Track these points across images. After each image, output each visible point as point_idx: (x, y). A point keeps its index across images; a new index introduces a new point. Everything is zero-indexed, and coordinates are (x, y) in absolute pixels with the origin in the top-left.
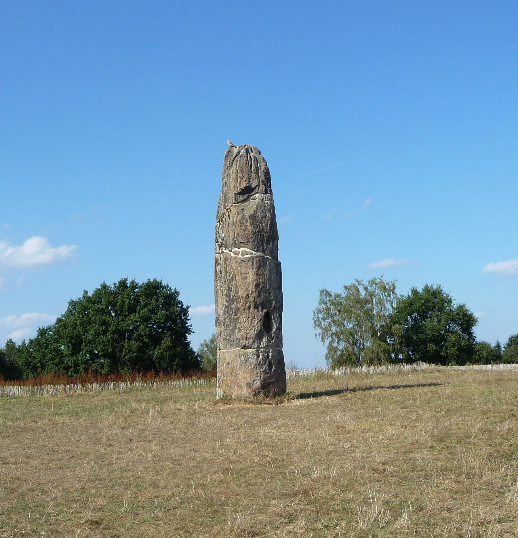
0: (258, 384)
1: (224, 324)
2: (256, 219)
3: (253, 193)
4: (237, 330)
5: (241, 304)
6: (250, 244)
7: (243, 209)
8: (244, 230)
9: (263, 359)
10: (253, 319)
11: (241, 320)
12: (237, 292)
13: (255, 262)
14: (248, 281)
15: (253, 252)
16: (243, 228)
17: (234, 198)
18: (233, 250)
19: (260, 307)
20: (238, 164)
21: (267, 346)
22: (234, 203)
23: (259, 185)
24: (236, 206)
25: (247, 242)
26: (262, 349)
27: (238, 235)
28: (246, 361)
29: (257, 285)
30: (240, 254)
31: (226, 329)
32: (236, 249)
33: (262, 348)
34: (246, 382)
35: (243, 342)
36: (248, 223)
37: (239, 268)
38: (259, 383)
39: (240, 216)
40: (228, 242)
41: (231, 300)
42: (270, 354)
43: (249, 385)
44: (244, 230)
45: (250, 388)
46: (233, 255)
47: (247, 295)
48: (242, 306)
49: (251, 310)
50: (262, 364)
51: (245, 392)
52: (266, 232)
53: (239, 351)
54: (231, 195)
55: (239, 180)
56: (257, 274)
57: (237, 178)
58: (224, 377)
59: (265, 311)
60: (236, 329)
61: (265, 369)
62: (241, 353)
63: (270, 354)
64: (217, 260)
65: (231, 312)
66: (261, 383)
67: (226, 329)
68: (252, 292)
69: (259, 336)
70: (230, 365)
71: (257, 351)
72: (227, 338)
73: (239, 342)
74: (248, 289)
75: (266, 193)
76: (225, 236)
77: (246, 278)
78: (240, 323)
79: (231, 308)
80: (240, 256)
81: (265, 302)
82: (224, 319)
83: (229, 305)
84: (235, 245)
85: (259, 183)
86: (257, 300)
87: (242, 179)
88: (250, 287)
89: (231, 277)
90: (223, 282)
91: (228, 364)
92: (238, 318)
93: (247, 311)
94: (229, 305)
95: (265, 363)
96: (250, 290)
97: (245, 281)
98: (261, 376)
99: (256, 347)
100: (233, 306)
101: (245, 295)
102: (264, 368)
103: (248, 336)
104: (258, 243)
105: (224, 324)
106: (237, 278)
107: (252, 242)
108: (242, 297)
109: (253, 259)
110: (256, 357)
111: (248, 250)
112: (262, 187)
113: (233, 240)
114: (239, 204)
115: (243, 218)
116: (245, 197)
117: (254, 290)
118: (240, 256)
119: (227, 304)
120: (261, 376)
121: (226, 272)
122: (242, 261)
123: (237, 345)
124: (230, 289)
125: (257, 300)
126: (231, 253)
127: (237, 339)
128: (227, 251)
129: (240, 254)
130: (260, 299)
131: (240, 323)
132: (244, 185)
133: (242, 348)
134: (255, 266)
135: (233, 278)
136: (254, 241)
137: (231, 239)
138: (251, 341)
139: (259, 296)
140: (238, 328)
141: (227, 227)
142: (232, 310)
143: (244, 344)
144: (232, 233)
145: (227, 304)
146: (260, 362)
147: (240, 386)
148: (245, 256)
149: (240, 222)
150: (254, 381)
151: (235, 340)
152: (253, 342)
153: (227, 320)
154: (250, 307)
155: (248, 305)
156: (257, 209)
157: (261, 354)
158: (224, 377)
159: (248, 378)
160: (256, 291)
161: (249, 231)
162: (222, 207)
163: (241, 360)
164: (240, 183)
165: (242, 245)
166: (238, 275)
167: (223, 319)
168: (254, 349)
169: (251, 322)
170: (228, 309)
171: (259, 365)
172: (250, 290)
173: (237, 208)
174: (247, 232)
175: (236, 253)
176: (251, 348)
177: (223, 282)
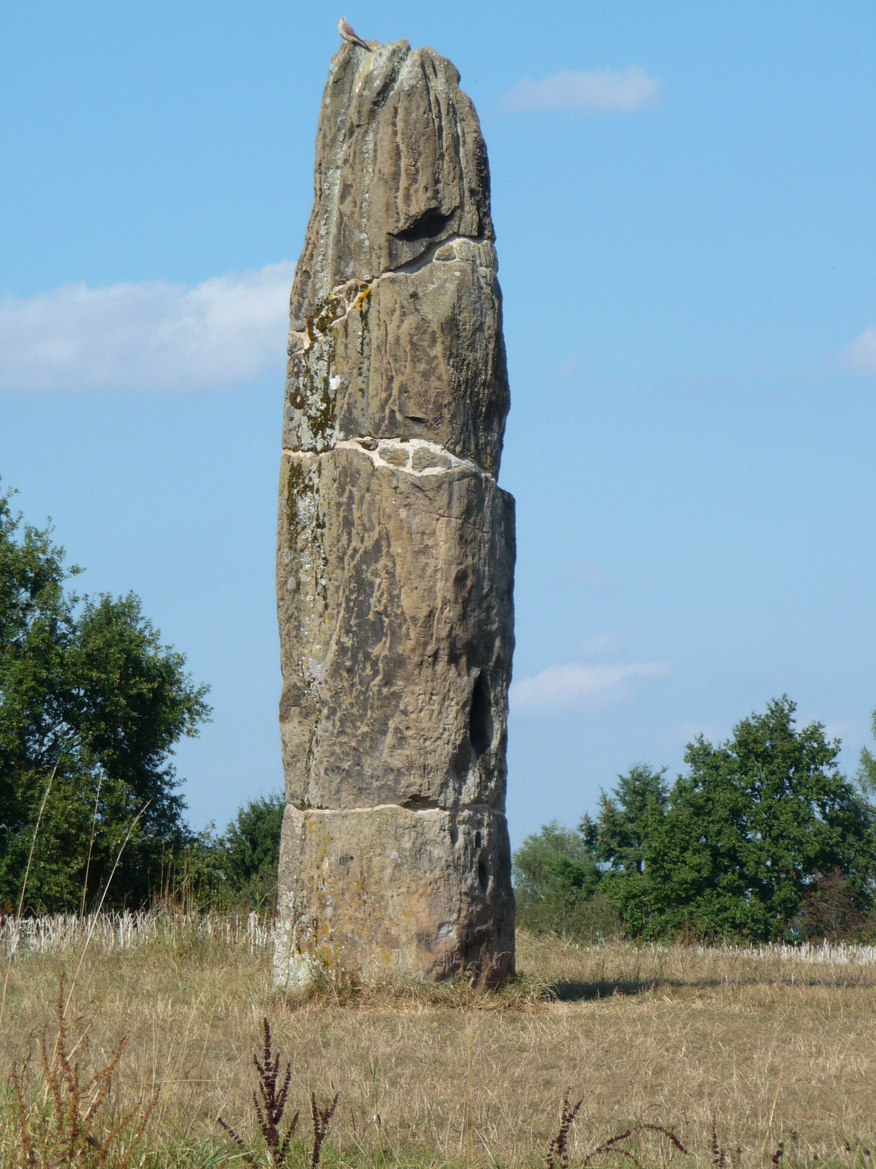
0: (451, 937)
1: (333, 711)
2: (458, 336)
3: (443, 236)
4: (389, 739)
5: (410, 644)
6: (444, 429)
7: (414, 296)
8: (426, 375)
9: (466, 848)
10: (444, 699)
11: (408, 701)
12: (394, 599)
13: (456, 495)
14: (432, 562)
15: (453, 458)
16: (422, 367)
17: (384, 252)
18: (383, 444)
19: (464, 660)
20: (400, 125)
21: (477, 801)
22: (387, 270)
23: (461, 206)
24: (393, 281)
25: (435, 420)
26: (466, 813)
27: (403, 389)
28: (419, 851)
29: (460, 579)
30: (410, 462)
31: (342, 733)
32: (395, 444)
33: (466, 806)
34: (414, 929)
35: (414, 783)
36: (438, 350)
37: (403, 513)
38: (453, 935)
39: (411, 321)
40: (356, 413)
41: (365, 625)
42: (485, 832)
43: (425, 940)
44: (426, 375)
45: (429, 950)
46: (379, 462)
47: (431, 614)
48: (413, 650)
49: (441, 666)
50: (465, 866)
51: (410, 961)
52: (484, 384)
53: (394, 814)
54: (372, 235)
55: (403, 182)
56: (461, 537)
57: (396, 176)
58: (323, 906)
59: (475, 672)
60: (384, 732)
61: (472, 887)
62: (401, 821)
63: (485, 832)
64: (296, 472)
65: (369, 671)
66: (460, 936)
67: (342, 733)
68: (445, 603)
69: (458, 768)
70: (354, 865)
71: (453, 818)
72: (346, 765)
73: (397, 781)
74: (431, 590)
75: (479, 236)
76: (344, 388)
77: (425, 550)
78: (405, 713)
79: (367, 656)
80: (408, 469)
81: (475, 642)
82: (336, 695)
83: (361, 645)
84: (392, 428)
85: (462, 197)
86: (458, 631)
87: (415, 181)
88: (440, 585)
89: (369, 544)
90: (332, 559)
91: (345, 859)
92: (397, 696)
93: (427, 672)
94: (361, 645)
95: (472, 863)
96: (439, 595)
97: (423, 560)
98: (460, 911)
99: (450, 802)
100: (379, 650)
101: (425, 612)
102: (469, 882)
103: (431, 761)
104: (465, 424)
105: (333, 711)
106: (396, 549)
107: (451, 422)
108: (414, 619)
109: (451, 483)
110: (448, 840)
111: (436, 449)
112: (470, 215)
113: (382, 407)
114: (401, 274)
115: (422, 327)
116: (420, 246)
117: (450, 596)
118: (408, 469)
119: (348, 642)
120: (460, 911)
121: (348, 523)
122: (418, 487)
123: (389, 793)
124: (362, 586)
125: (458, 631)
126: (375, 455)
127: (389, 770)
128: (352, 445)
129: (410, 462)
130: (465, 630)
131: (405, 713)
132: (419, 205)
133: (406, 805)
134: (457, 508)
135: (377, 546)
136: (453, 416)
137: (375, 404)
138: (438, 779)
139: (463, 617)
140: (397, 729)
141: (353, 353)
142: (375, 664)
143: (414, 790)
144: (376, 382)
145: (348, 642)
146: (459, 858)
147: (392, 943)
148: (428, 471)
149: (413, 344)
150: (440, 926)
151: (380, 773)
152: (444, 785)
153: (347, 700)
154: (435, 656)
155: (431, 649)
156: (459, 298)
157: (461, 828)
158: (323, 906)
159: (423, 916)
160: (456, 602)
161: (439, 379)
162: (325, 278)
163: (400, 850)
164: (407, 198)
165: (417, 428)
166: (399, 538)
167: (326, 695)
168: (444, 808)
169: (440, 713)
170: (354, 658)
171: (456, 869)
172: (439, 595)
173: (397, 288)
174: (434, 383)
175: (397, 458)
176: (434, 804)
177: (332, 559)
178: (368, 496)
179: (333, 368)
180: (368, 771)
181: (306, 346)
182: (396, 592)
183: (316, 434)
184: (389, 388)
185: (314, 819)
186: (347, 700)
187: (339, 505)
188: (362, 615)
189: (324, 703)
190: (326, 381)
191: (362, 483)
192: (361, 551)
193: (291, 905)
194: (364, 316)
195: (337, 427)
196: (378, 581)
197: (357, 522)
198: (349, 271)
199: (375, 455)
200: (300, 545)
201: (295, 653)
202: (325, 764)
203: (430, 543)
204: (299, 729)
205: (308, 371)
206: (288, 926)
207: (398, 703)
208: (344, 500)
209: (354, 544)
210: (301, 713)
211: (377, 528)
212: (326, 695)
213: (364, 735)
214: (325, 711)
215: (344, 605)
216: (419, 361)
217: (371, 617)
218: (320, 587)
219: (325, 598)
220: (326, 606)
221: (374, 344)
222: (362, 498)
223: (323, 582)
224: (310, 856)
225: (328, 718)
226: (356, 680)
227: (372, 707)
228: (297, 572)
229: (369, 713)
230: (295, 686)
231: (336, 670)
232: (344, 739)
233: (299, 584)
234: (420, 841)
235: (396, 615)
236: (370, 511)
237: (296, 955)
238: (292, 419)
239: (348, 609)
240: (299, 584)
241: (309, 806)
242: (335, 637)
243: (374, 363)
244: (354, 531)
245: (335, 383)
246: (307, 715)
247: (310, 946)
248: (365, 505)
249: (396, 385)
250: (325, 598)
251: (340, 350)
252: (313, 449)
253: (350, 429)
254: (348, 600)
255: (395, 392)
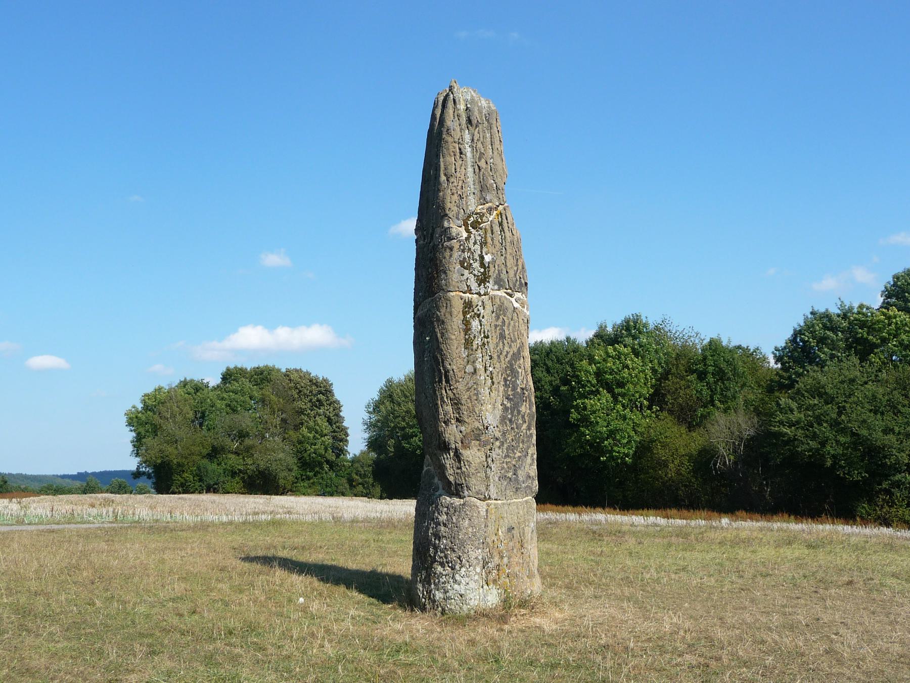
1: (502, 444)
31: (507, 456)
40: (502, 276)
46: (516, 305)
58: (502, 557)
60: (526, 456)
65: (520, 421)
67: (507, 456)
72: (510, 475)
76: (493, 261)
79: (519, 412)
82: (504, 434)
90: (495, 356)
105: (502, 444)
121: (502, 337)
126: (513, 300)
128: (501, 293)
137: (512, 273)
142: (523, 417)
153: (510, 437)
170: (512, 413)
177: (495, 356)
178: (512, 323)
179: (485, 250)
180: (521, 478)
181: (465, 235)
183: (479, 285)
184: (517, 265)
185: (492, 506)
186: (510, 437)
187: (496, 326)
188: (514, 389)
189: (497, 439)
190: (482, 257)
191: (509, 314)
192: (511, 353)
193: (480, 558)
194: (501, 224)
195: (491, 281)
196: (520, 370)
197: (507, 336)
198: (488, 198)
199: (513, 300)
200: (475, 347)
201: (476, 410)
202: (499, 474)
204: (479, 454)
205: (470, 249)
206: (478, 570)
208: (499, 323)
209: (506, 348)
210: (480, 445)
211: (518, 341)
212: (498, 435)
213: (519, 457)
214: (498, 443)
215: (502, 383)
217: (519, 390)
218: (488, 372)
219: (492, 378)
220: (493, 383)
221: (508, 239)
222: (509, 324)
223: (491, 369)
224: (491, 529)
225: (499, 447)
226: (514, 426)
227: (523, 442)
228: (474, 362)
229: (521, 445)
230: (478, 429)
231: (503, 419)
232: (508, 460)
233: (475, 370)
236: (513, 331)
237: (485, 587)
238: (463, 275)
239: (506, 385)
240: (475, 370)
241: (490, 498)
242: (499, 402)
243: (509, 251)
244: (505, 342)
245: (488, 258)
246: (484, 445)
247: (495, 581)
248: (511, 328)
249: (520, 263)
250: (492, 378)
251: (489, 240)
252: (479, 294)
253: (499, 283)
254: (505, 380)
255: (520, 267)
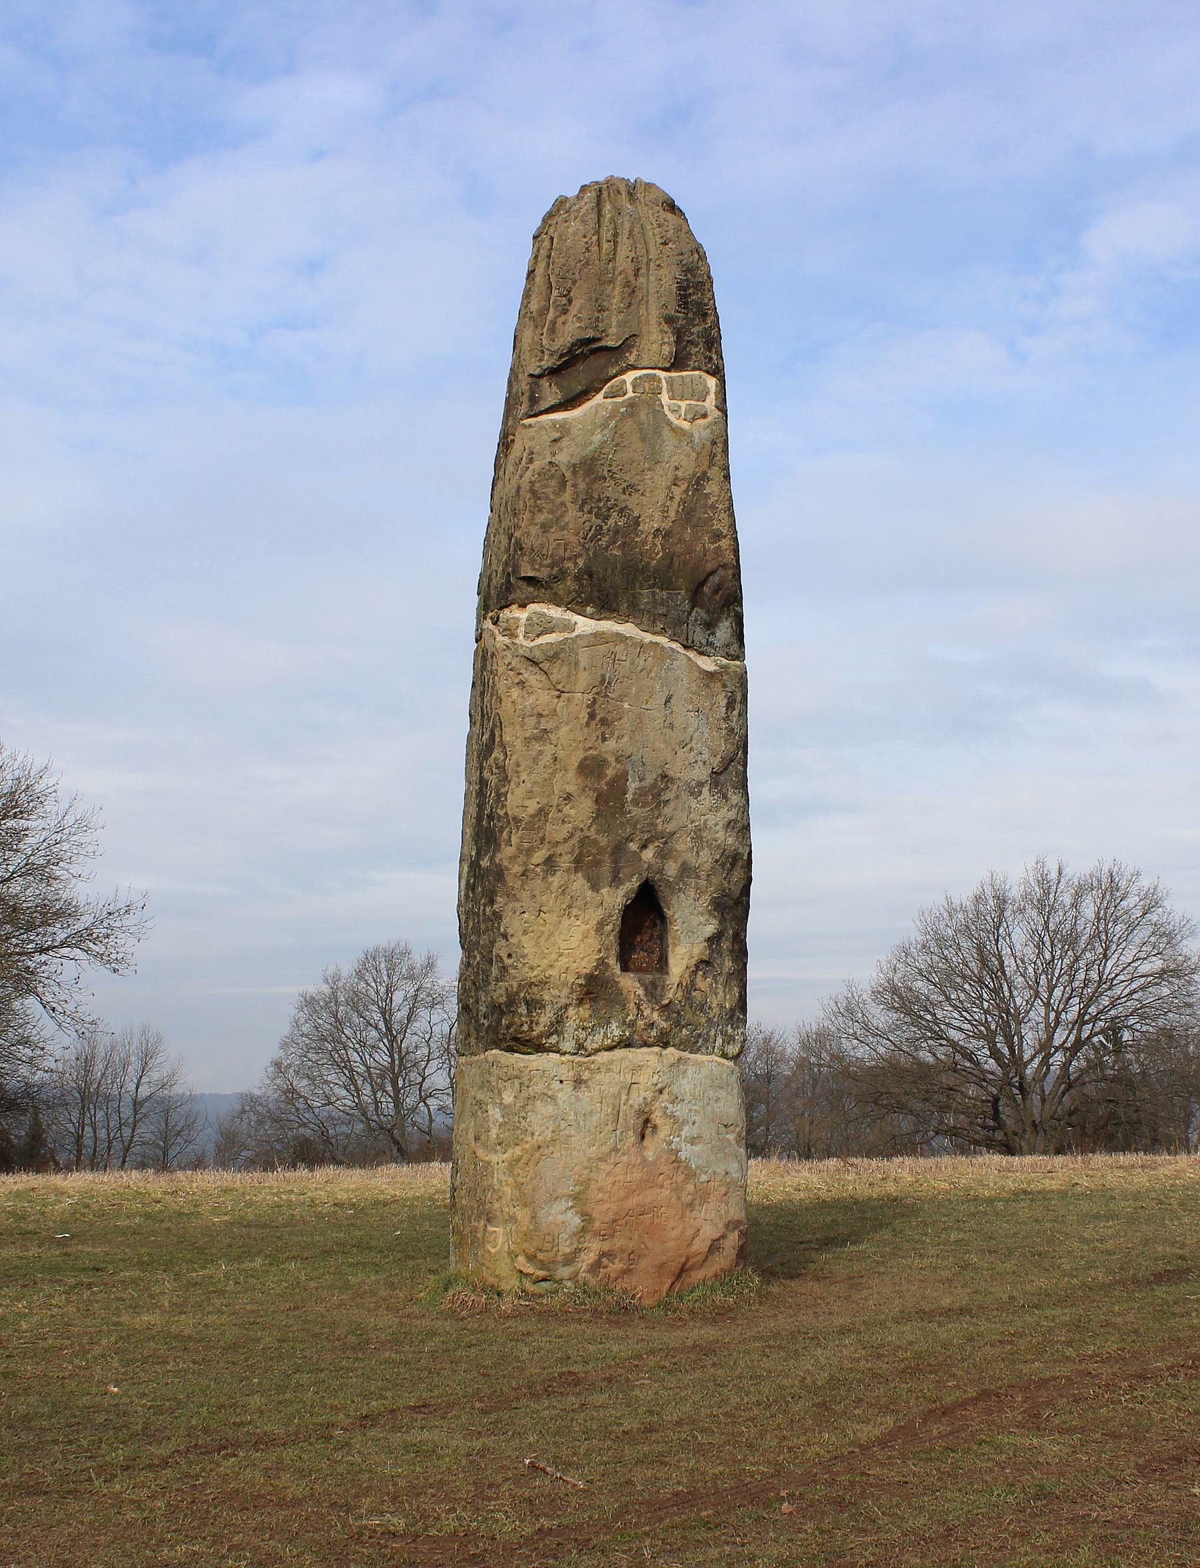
16: (541, 518)
148: (543, 640)
149: (533, 492)
182: (503, 790)
203: (549, 726)
207: (499, 924)
216: (540, 511)
234: (524, 1094)
235: (499, 816)
